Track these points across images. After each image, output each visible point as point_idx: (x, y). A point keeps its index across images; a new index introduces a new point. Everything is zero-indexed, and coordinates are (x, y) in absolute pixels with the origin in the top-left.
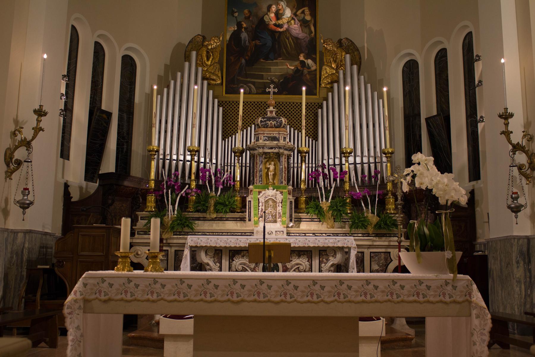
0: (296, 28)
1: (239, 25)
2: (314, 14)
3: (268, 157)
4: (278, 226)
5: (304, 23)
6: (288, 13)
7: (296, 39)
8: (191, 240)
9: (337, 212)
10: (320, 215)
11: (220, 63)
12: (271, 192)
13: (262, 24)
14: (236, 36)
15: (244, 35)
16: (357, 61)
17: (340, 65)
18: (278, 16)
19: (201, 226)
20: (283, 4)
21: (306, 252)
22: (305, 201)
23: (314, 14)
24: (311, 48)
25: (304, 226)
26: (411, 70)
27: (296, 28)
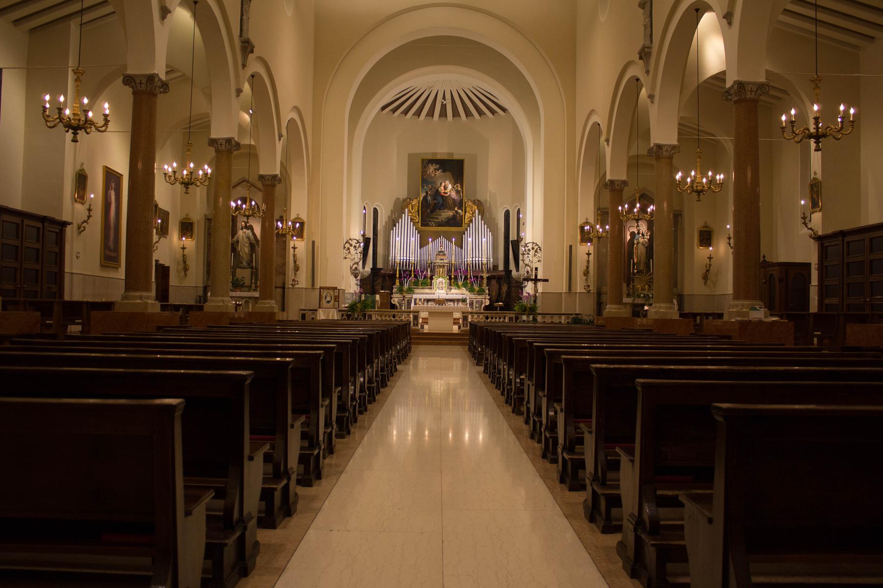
0: (454, 195)
1: (427, 193)
2: (462, 187)
3: (440, 266)
4: (444, 291)
5: (458, 192)
6: (450, 187)
7: (454, 200)
8: (415, 296)
9: (465, 285)
10: (458, 287)
11: (418, 211)
12: (441, 279)
13: (437, 192)
14: (425, 198)
15: (429, 198)
16: (482, 213)
17: (474, 213)
18: (445, 188)
19: (416, 291)
20: (447, 182)
21: (451, 300)
22: (453, 281)
23: (462, 187)
24: (460, 204)
25: (453, 291)
26: (507, 214)
27: (454, 195)
